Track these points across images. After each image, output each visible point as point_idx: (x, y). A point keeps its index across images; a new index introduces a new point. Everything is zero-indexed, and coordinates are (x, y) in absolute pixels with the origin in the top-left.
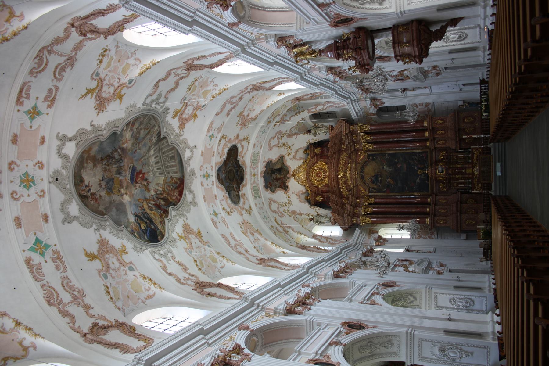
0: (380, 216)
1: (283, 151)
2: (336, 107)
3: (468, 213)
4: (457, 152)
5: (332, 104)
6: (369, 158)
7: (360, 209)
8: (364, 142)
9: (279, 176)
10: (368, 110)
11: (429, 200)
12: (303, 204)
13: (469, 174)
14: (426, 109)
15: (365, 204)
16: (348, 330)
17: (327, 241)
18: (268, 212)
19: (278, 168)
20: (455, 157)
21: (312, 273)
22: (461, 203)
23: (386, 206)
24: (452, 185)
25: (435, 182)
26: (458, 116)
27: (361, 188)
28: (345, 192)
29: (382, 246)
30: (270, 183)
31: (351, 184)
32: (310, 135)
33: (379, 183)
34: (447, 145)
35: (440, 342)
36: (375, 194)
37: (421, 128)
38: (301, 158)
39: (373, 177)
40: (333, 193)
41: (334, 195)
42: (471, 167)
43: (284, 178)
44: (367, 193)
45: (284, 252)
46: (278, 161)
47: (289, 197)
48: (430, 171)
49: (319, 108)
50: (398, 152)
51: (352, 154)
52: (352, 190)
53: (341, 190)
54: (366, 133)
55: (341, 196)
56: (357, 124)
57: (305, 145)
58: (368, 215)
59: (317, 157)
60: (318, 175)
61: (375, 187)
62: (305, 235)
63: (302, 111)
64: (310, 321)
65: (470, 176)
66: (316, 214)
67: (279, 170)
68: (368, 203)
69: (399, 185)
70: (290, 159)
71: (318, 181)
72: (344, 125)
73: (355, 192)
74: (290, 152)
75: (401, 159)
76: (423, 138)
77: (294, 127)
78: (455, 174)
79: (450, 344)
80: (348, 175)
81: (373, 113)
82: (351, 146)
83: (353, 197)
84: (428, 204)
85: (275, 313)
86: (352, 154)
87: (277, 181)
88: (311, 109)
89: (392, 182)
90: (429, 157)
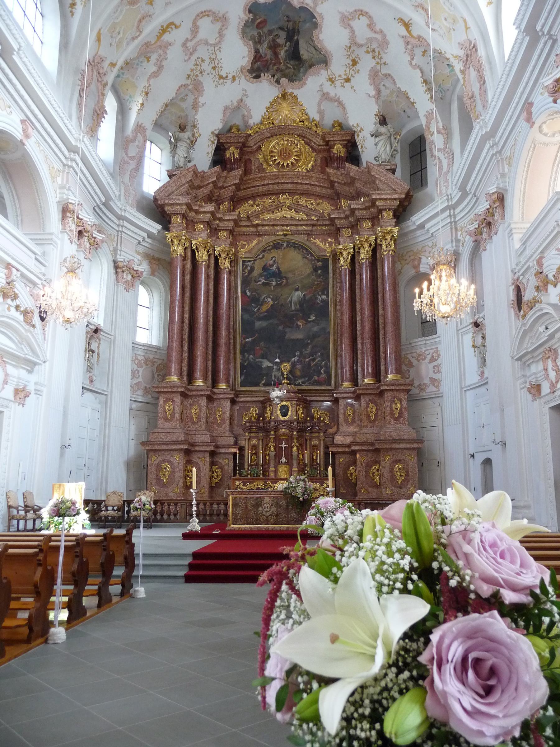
4: (327, 447)
5: (445, 169)
6: (319, 261)
7: (204, 235)
9: (282, 53)
10: (427, 254)
11: (223, 386)
12: (221, 116)
13: (276, 472)
14: (427, 381)
15: (217, 248)
17: (132, 158)
19: (302, 51)
20: (315, 442)
23: (212, 292)
24: (252, 435)
25: (262, 399)
27: (255, 242)
28: (245, 209)
29: (113, 276)
30: (264, 22)
32: (375, 124)
37: (382, 368)
38: (321, 113)
39: (278, 268)
41: (237, 181)
45: (73, 5)
47: (234, 78)
50: (332, 322)
51: (328, 222)
53: (251, 202)
56: (397, 224)
57: (352, 121)
59: (325, 150)
60: (285, 153)
61: (256, 273)
62: (142, 104)
65: (272, 474)
68: (220, 255)
71: (272, 152)
73: (245, 229)
74: (338, 83)
75: (315, 329)
78: (278, 439)
81: (419, 264)
83: (231, 224)
84: (215, 383)
87: (270, 48)
89: (265, 308)
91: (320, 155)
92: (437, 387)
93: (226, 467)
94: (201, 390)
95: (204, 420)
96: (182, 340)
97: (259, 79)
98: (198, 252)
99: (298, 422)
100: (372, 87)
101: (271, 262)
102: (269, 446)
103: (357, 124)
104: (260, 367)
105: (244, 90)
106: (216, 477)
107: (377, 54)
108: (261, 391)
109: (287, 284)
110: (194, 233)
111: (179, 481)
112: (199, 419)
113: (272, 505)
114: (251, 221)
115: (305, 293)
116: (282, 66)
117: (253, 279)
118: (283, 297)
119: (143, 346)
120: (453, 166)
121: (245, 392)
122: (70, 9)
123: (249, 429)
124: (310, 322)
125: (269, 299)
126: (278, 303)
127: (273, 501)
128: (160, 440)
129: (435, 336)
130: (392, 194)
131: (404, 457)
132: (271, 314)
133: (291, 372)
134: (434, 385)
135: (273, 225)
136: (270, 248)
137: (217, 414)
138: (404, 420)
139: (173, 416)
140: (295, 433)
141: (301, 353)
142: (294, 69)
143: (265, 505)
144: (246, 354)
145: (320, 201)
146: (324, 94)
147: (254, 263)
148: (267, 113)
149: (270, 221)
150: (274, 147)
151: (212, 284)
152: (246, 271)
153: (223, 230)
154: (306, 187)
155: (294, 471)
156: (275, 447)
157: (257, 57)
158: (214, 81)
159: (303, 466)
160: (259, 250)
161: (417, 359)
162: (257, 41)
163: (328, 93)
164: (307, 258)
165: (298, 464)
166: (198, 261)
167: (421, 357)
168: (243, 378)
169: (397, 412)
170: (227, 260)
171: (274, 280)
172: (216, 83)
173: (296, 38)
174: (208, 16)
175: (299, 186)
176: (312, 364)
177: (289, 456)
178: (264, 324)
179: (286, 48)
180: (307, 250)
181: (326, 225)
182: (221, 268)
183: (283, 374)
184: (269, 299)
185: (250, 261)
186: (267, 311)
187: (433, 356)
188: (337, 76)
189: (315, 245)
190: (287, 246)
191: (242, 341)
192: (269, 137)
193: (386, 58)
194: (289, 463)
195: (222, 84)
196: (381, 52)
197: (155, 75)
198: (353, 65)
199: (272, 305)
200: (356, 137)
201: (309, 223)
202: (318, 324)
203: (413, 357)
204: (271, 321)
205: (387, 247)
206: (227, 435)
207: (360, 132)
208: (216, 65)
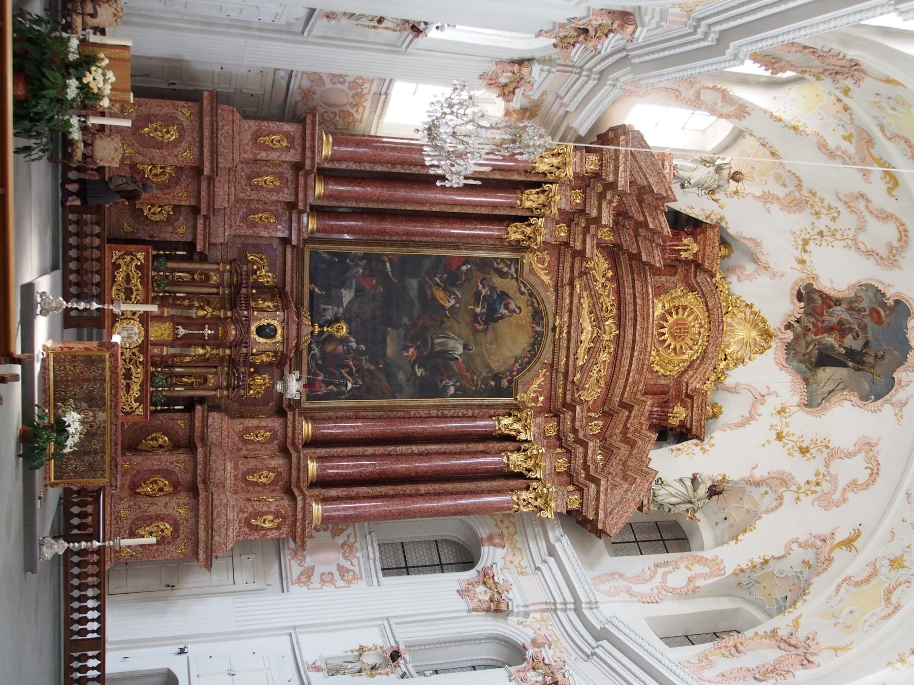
2: (621, 576)
4: (202, 400)
5: (637, 588)
6: (510, 382)
7: (564, 206)
9: (830, 339)
10: (510, 557)
14: (309, 561)
15: (541, 222)
17: (698, 95)
19: (829, 370)
20: (212, 381)
22: (195, 210)
24: (227, 275)
25: (288, 289)
26: (197, 546)
28: (600, 265)
29: (507, 56)
30: (879, 321)
33: (484, 292)
34: (238, 425)
37: (333, 492)
38: (734, 390)
39: (502, 317)
41: (644, 258)
42: (155, 344)
44: (529, 259)
47: (802, 262)
48: (306, 331)
51: (568, 398)
52: (576, 273)
53: (610, 274)
59: (679, 391)
60: (680, 331)
61: (497, 281)
62: (780, 120)
63: (742, 570)
67: (825, 359)
68: (530, 225)
69: (414, 283)
70: (776, 393)
73: (568, 265)
74: (776, 420)
75: (401, 376)
76: (322, 451)
78: (215, 322)
80: (587, 326)
81: (495, 545)
83: (578, 246)
84: (318, 211)
87: (840, 322)
88: (705, 576)
89: (440, 295)
92: (299, 581)
93: (170, 229)
94: (306, 195)
96: (394, 164)
97: (796, 301)
98: (538, 193)
99: (246, 355)
100: (766, 475)
101: (512, 306)
102: (206, 308)
103: (713, 445)
104: (342, 285)
105: (782, 276)
106: (152, 211)
107: (813, 488)
108: (303, 286)
110: (569, 188)
111: (144, 156)
112: (257, 188)
113: (91, 426)
114: (580, 276)
115: (460, 360)
116: (811, 337)
117: (488, 276)
118: (456, 325)
119: (386, 94)
120: (639, 602)
121: (299, 259)
123: (237, 272)
124: (413, 368)
127: (99, 427)
128: (220, 124)
129: (380, 573)
130: (605, 510)
131: (182, 536)
132: (430, 304)
134: (302, 574)
135: (570, 311)
137: (265, 215)
138: (246, 534)
139: (265, 147)
140: (228, 352)
141: (363, 353)
142: (805, 355)
143: (91, 414)
144: (365, 262)
149: (578, 308)
150: (692, 312)
151: (484, 211)
152: (501, 265)
153: (569, 231)
154: (626, 362)
155: (162, 350)
156: (204, 317)
157: (829, 301)
158: (801, 231)
159: (170, 362)
160: (533, 287)
161: (345, 543)
162: (852, 305)
164: (514, 365)
165: (175, 356)
166: (522, 192)
167: (348, 550)
168: (325, 256)
169: (258, 523)
170: (520, 237)
171: (484, 310)
172: (798, 233)
173: (850, 364)
174: (900, 240)
175: (628, 353)
176: (343, 371)
177: (188, 342)
178: (413, 293)
179: (837, 346)
180: (529, 363)
181: (565, 394)
182: (508, 226)
183: (330, 323)
184: (453, 302)
186: (434, 298)
187: (348, 571)
188: (787, 420)
189: (535, 376)
190: (536, 332)
192: (707, 305)
193: (806, 500)
194: (176, 341)
195: (796, 241)
197: (823, 146)
198: (800, 448)
199: (443, 306)
200: (695, 441)
201: (571, 369)
202: (408, 380)
203: (348, 537)
204: (417, 304)
205: (524, 500)
207: (702, 449)
208: (825, 238)
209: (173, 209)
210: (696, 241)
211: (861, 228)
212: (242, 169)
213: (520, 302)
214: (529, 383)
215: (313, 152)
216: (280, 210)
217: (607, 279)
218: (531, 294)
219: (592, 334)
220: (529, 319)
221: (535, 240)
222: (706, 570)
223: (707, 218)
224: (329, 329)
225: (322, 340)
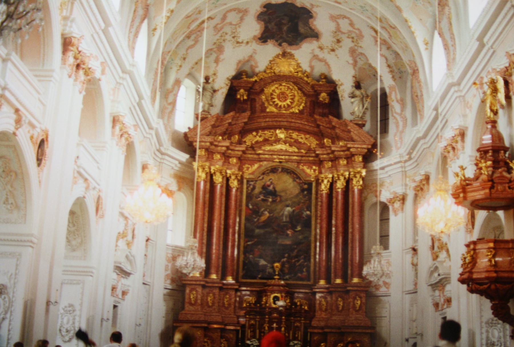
0: (207, 196)
1: (326, 39)
3: (205, 340)
4: (306, 328)
6: (305, 184)
7: (220, 163)
8: (333, 178)
11: (230, 280)
14: (381, 283)
15: (229, 172)
16: (37, 139)
17: (170, 104)
18: (225, 7)
20: (297, 324)
21: (123, 79)
23: (223, 206)
24: (251, 317)
25: (258, 289)
28: (250, 139)
31: (264, 150)
32: (352, 86)
33: (262, 197)
35: (15, 287)
36: (245, 191)
37: (349, 272)
38: (312, 67)
39: (274, 188)
40: (250, 118)
41: (246, 120)
43: (281, 38)
44: (247, 176)
45: (155, 29)
46: (310, 28)
47: (247, 43)
49: (395, 106)
50: (313, 233)
51: (313, 155)
52: (253, 152)
53: (254, 133)
54: (348, 181)
55: (244, 132)
56: (364, 167)
57: (335, 77)
58: (211, 176)
60: (283, 96)
61: (257, 190)
63: (393, 77)
64: (52, 76)
66: (216, 86)
68: (230, 177)
69: (257, 231)
70: (313, 50)
72: (365, 146)
73: (249, 156)
74: (326, 51)
75: (300, 237)
76: (333, 275)
77: (368, 60)
79: (11, 303)
82: (328, 154)
84: (223, 277)
85: (65, 18)
86: (313, 155)
87: (276, 25)
89: (263, 218)
90: (300, 282)
91: (310, 99)
95: (216, 305)
96: (202, 243)
97: (267, 43)
98: (215, 175)
100: (351, 58)
101: (269, 183)
104: (257, 264)
108: (257, 283)
109: (281, 201)
112: (213, 303)
115: (294, 209)
116: (284, 35)
117: (255, 195)
119: (172, 246)
122: (153, 32)
125: (266, 212)
126: (272, 216)
128: (187, 319)
129: (387, 251)
132: (267, 224)
133: (281, 270)
134: (385, 286)
135: (272, 155)
136: (268, 171)
137: (226, 300)
141: (289, 256)
145: (308, 136)
146: (314, 56)
147: (255, 183)
148: (270, 64)
151: (224, 199)
152: (250, 189)
153: (234, 157)
156: (268, 327)
163: (317, 56)
171: (271, 197)
172: (234, 46)
174: (235, 11)
176: (297, 264)
183: (274, 271)
184: (266, 212)
185: (252, 181)
186: (264, 222)
190: (282, 171)
191: (244, 244)
192: (271, 83)
196: (358, 40)
199: (269, 217)
204: (266, 230)
205: (357, 183)
206: (232, 316)
209: (222, 339)
210: (239, 90)
211: (231, 24)
212: (205, 309)
213: (267, 179)
214: (306, 174)
215: (198, 281)
216: (223, 293)
217: (257, 135)
218: (263, 174)
219: (282, 144)
220: (275, 175)
221: (237, 174)
222: (393, 93)
223: (227, 85)
224: (277, 271)
225: (282, 274)
